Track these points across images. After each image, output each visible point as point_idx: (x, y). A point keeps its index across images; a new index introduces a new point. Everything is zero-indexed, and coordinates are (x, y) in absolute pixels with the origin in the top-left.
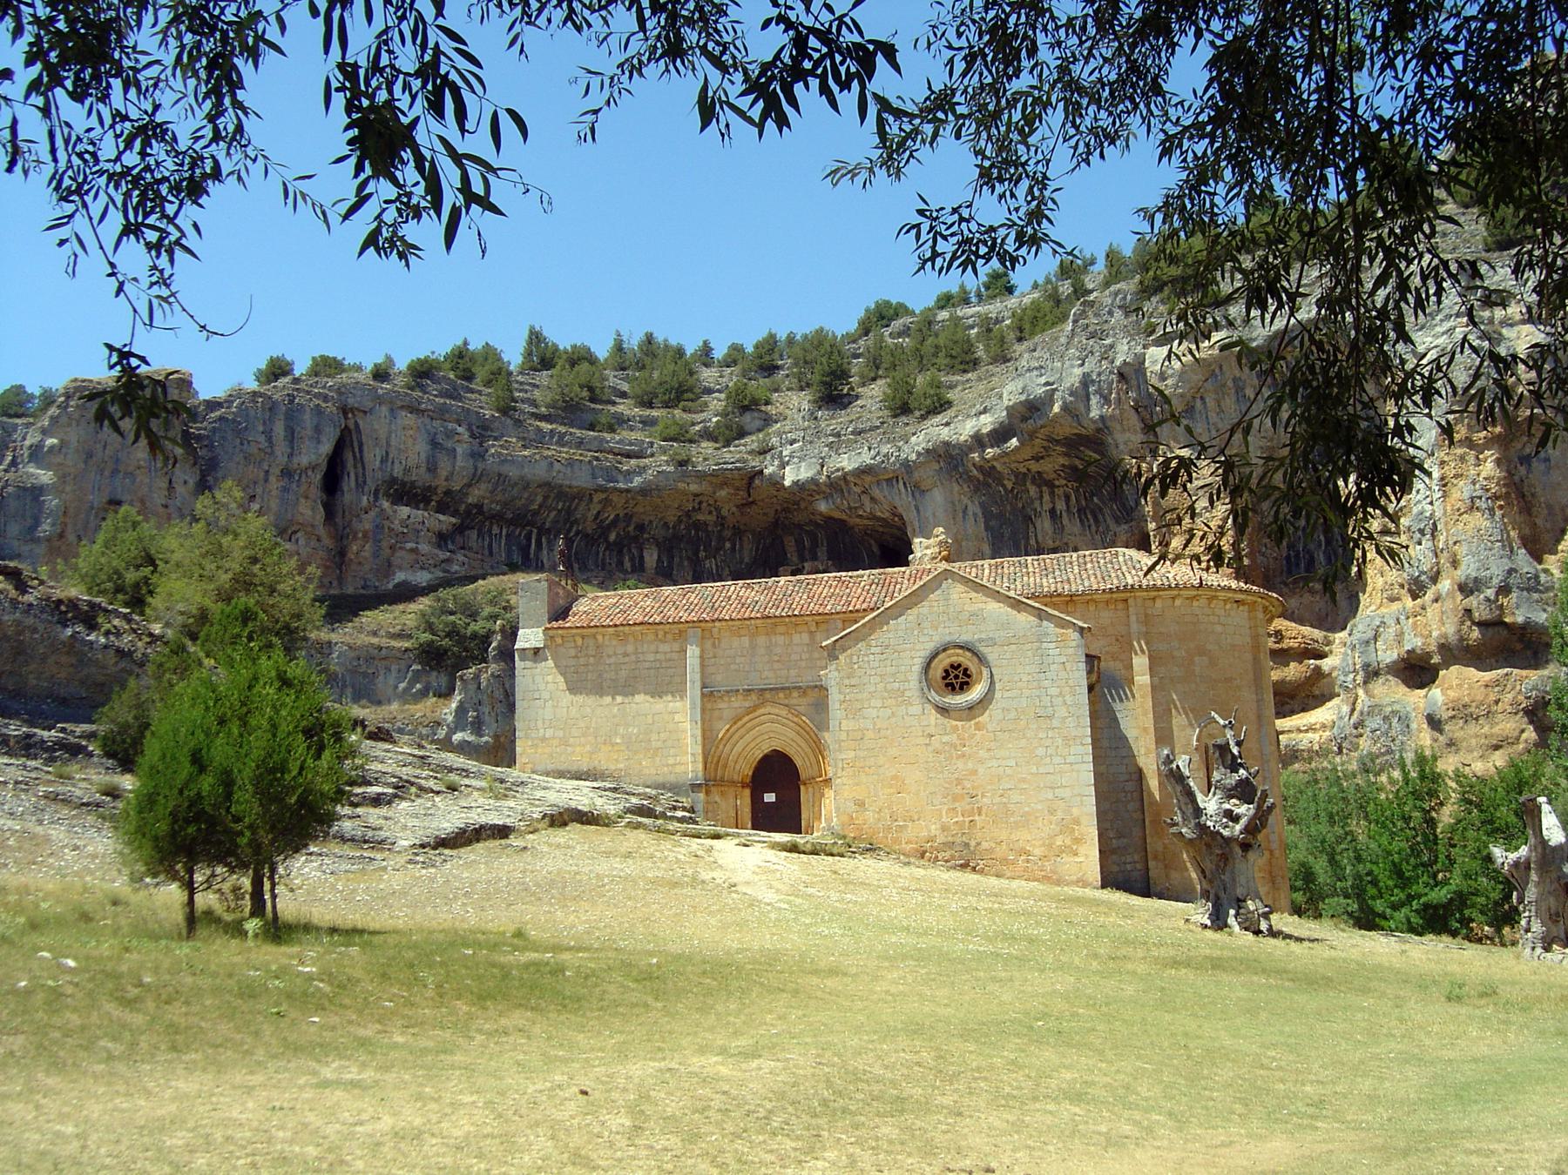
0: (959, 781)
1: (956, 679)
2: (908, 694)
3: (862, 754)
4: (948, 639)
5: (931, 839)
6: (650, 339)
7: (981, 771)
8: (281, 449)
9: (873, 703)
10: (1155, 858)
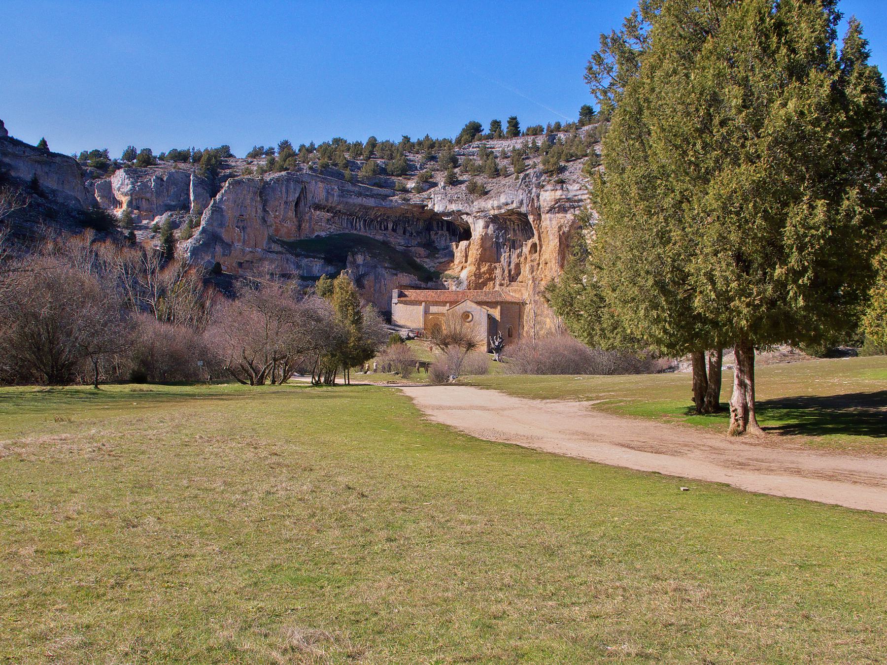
8: (284, 195)
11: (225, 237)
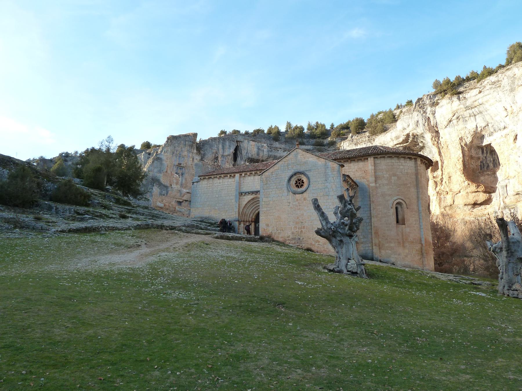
0: (298, 218)
1: (299, 184)
2: (283, 189)
3: (268, 209)
4: (296, 171)
5: (289, 237)
6: (317, 123)
7: (305, 214)
9: (273, 192)
10: (376, 245)
11: (163, 180)
